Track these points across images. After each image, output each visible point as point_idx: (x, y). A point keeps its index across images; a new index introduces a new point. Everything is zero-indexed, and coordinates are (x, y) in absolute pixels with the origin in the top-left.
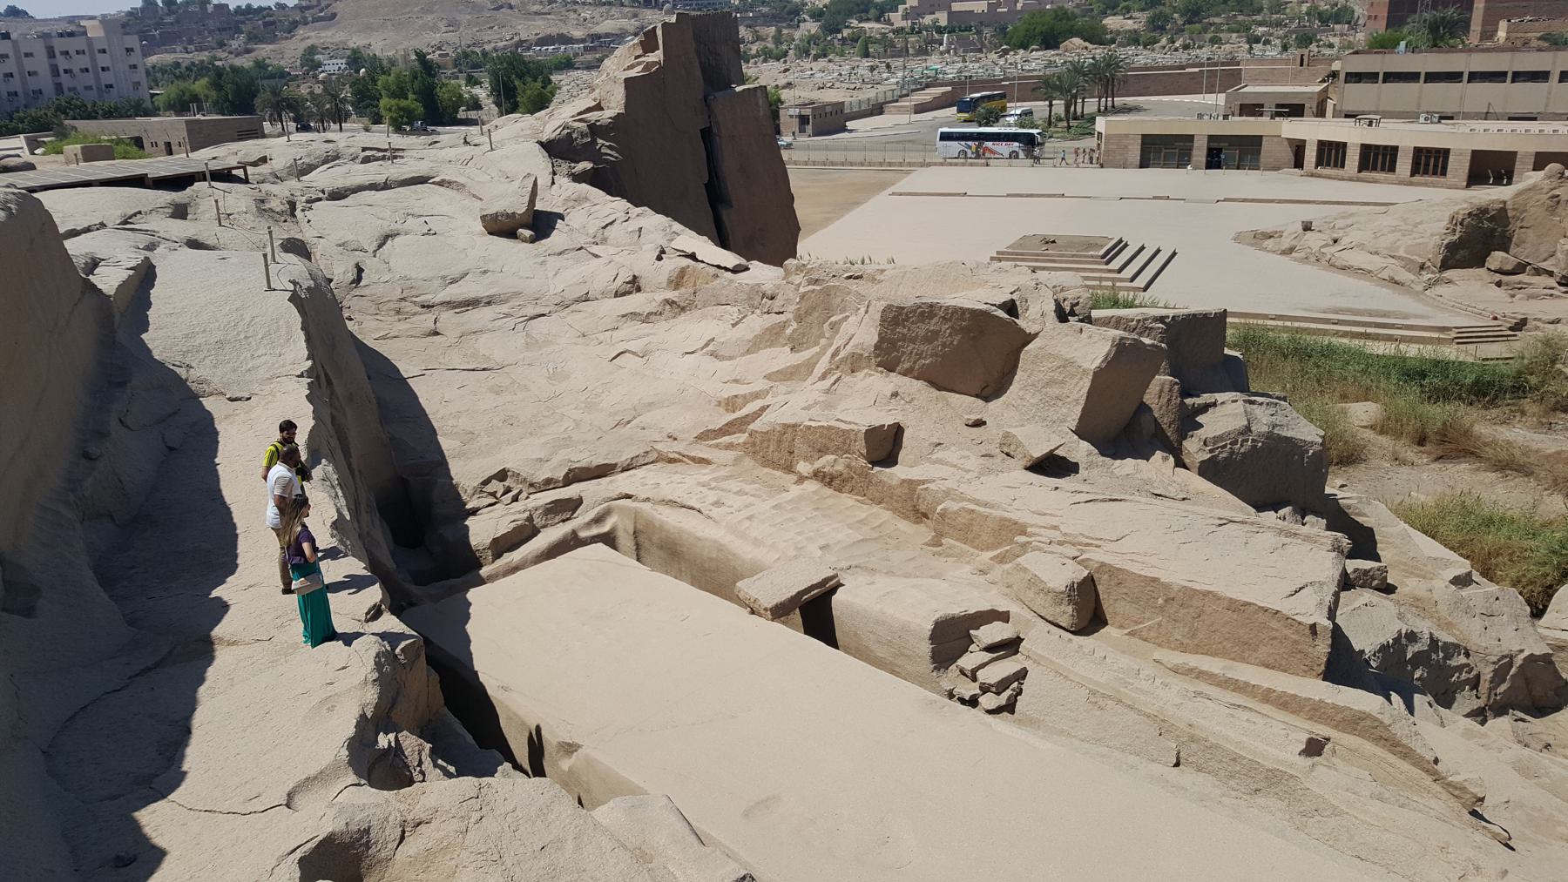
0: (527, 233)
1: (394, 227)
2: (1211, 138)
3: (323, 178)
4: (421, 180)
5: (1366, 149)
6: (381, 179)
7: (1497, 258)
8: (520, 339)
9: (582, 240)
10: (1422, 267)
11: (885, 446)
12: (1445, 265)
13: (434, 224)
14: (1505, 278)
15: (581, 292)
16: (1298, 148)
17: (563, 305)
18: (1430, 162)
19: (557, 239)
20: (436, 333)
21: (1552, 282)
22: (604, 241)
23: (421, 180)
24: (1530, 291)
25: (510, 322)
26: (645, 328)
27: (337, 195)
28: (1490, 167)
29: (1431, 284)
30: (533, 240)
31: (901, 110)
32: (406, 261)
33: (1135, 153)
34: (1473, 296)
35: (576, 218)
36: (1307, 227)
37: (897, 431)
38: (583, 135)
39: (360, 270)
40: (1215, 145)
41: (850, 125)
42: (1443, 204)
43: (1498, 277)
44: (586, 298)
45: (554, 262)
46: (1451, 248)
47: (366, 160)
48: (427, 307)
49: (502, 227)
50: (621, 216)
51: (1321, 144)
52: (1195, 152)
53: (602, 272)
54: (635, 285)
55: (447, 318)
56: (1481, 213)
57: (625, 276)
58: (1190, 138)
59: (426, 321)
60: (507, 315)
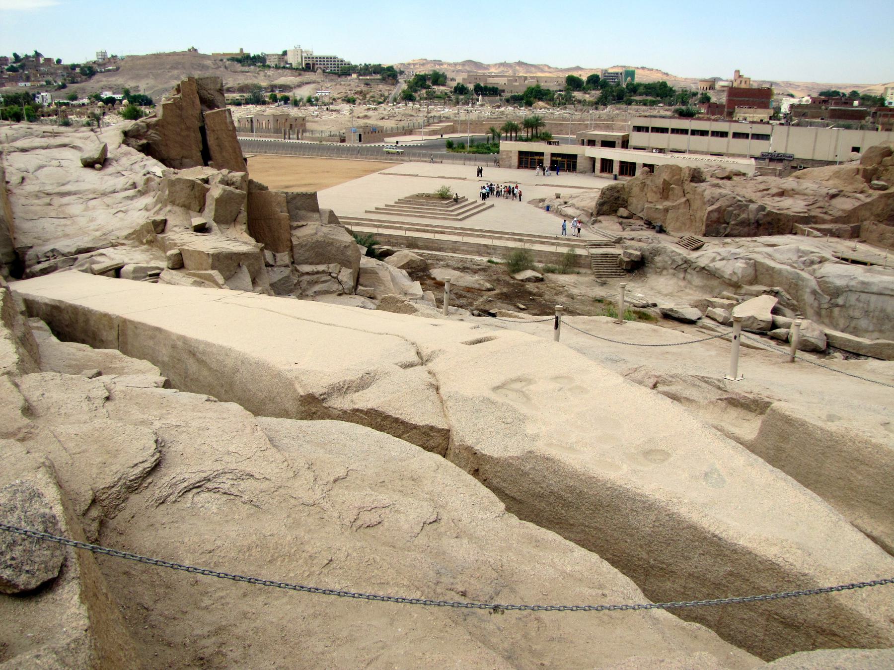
0: (98, 166)
1: (45, 163)
2: (553, 155)
3: (20, 144)
4: (65, 146)
5: (622, 163)
6: (45, 145)
7: (622, 211)
8: (82, 207)
9: (120, 169)
10: (592, 214)
11: (160, 226)
12: (599, 213)
13: (63, 163)
14: (625, 221)
15: (111, 189)
16: (593, 160)
17: (104, 194)
18: (607, 165)
19: (110, 170)
20: (50, 205)
21: (642, 223)
22: (131, 170)
23: (65, 146)
24: (633, 227)
25: (81, 201)
26: (129, 202)
27: (24, 150)
28: (628, 168)
29: (595, 222)
30: (100, 169)
31: (420, 133)
32: (47, 179)
33: (515, 160)
34: (610, 227)
35: (125, 161)
36: (558, 197)
37: (165, 222)
38: (143, 128)
39: (23, 179)
40: (554, 158)
41: (387, 139)
42: (602, 183)
43: (621, 220)
44: (114, 192)
45: (106, 178)
46: (601, 205)
47: (43, 137)
49: (89, 164)
50: (139, 160)
51: (603, 160)
52: (545, 162)
53: (120, 182)
54: (134, 185)
55: (57, 201)
56: (611, 189)
57: (131, 182)
58: (542, 154)
59: (47, 200)
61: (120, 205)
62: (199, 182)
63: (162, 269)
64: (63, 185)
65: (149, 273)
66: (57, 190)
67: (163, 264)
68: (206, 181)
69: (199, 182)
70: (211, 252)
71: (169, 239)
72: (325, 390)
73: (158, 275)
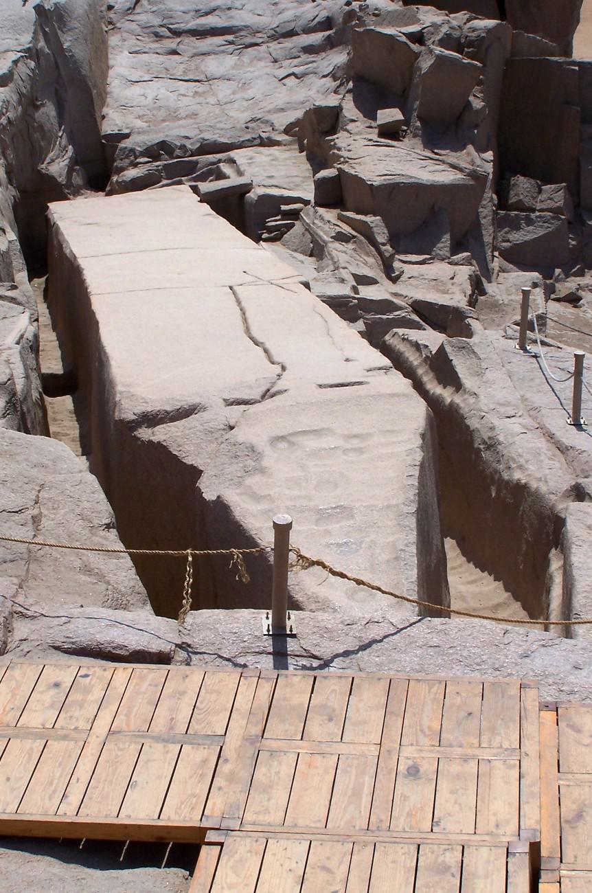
48: (176, 33)
59: (172, 44)
60: (231, 43)
61: (296, 61)
62: (404, 39)
63: (306, 203)
64: (207, 14)
65: (284, 207)
66: (192, 25)
67: (310, 195)
68: (418, 38)
69: (404, 39)
70: (377, 181)
71: (335, 147)
72: (134, 417)
73: (295, 215)
